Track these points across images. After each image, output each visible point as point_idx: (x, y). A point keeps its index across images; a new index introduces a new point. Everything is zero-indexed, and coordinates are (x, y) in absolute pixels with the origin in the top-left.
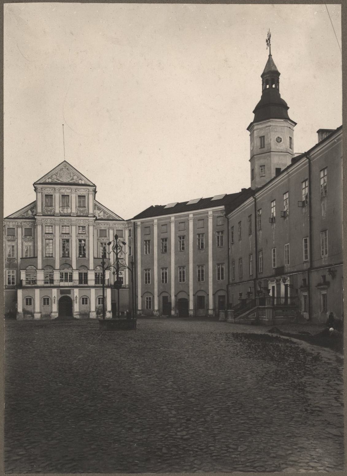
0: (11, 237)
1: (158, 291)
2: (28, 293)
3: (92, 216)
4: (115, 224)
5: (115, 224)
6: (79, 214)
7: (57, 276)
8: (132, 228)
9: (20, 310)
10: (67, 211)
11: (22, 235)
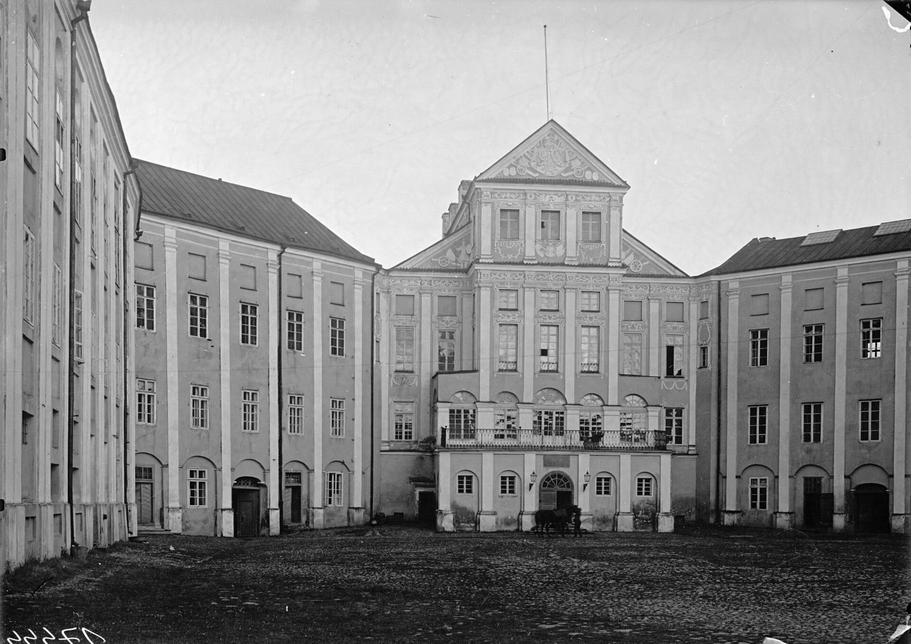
0: (404, 318)
1: (792, 462)
3: (617, 265)
4: (664, 286)
5: (664, 286)
6: (583, 262)
7: (526, 419)
8: (713, 299)
9: (444, 504)
10: (555, 252)
11: (432, 313)
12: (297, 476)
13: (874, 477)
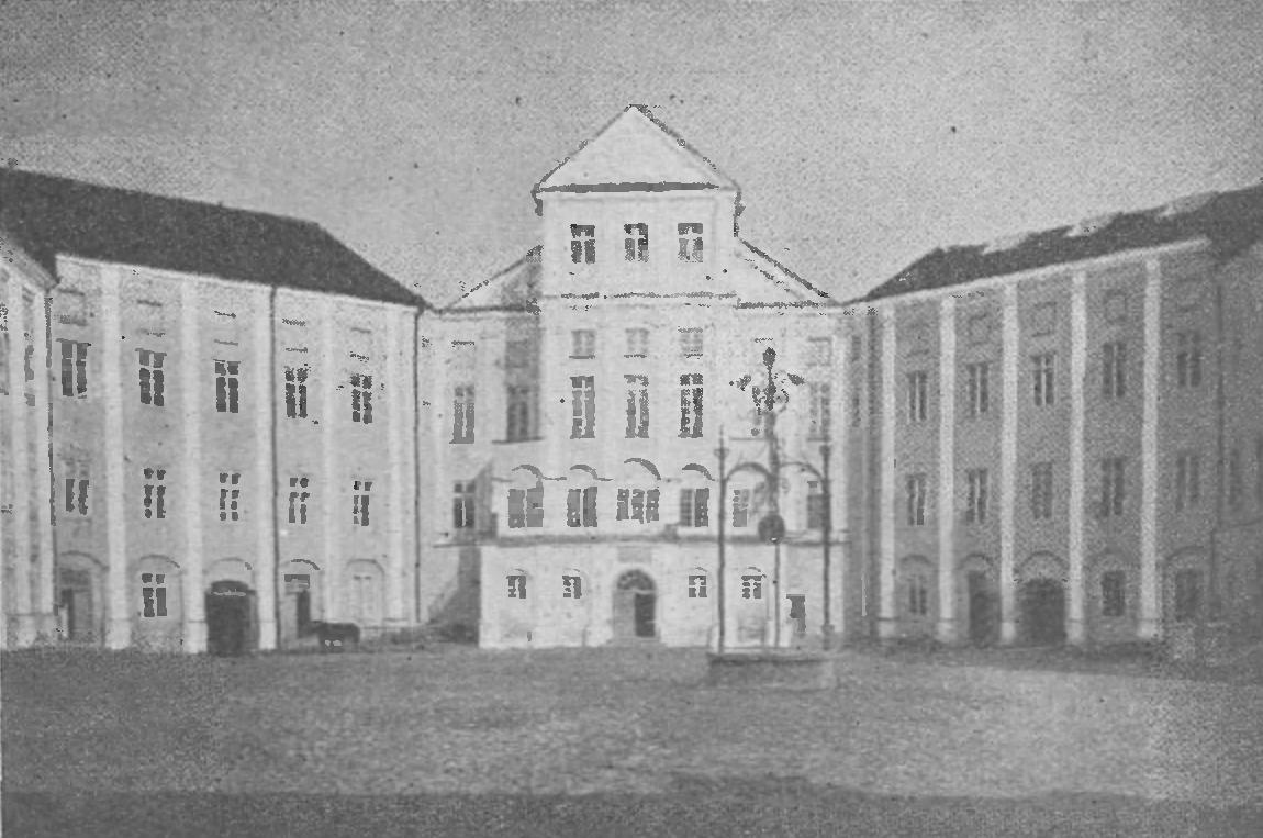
2: (514, 560)
12: (305, 578)
13: (1045, 571)
